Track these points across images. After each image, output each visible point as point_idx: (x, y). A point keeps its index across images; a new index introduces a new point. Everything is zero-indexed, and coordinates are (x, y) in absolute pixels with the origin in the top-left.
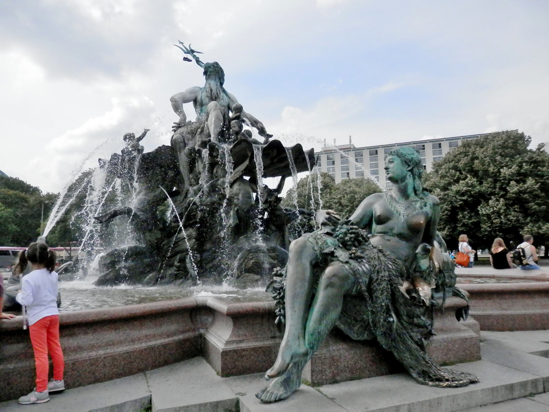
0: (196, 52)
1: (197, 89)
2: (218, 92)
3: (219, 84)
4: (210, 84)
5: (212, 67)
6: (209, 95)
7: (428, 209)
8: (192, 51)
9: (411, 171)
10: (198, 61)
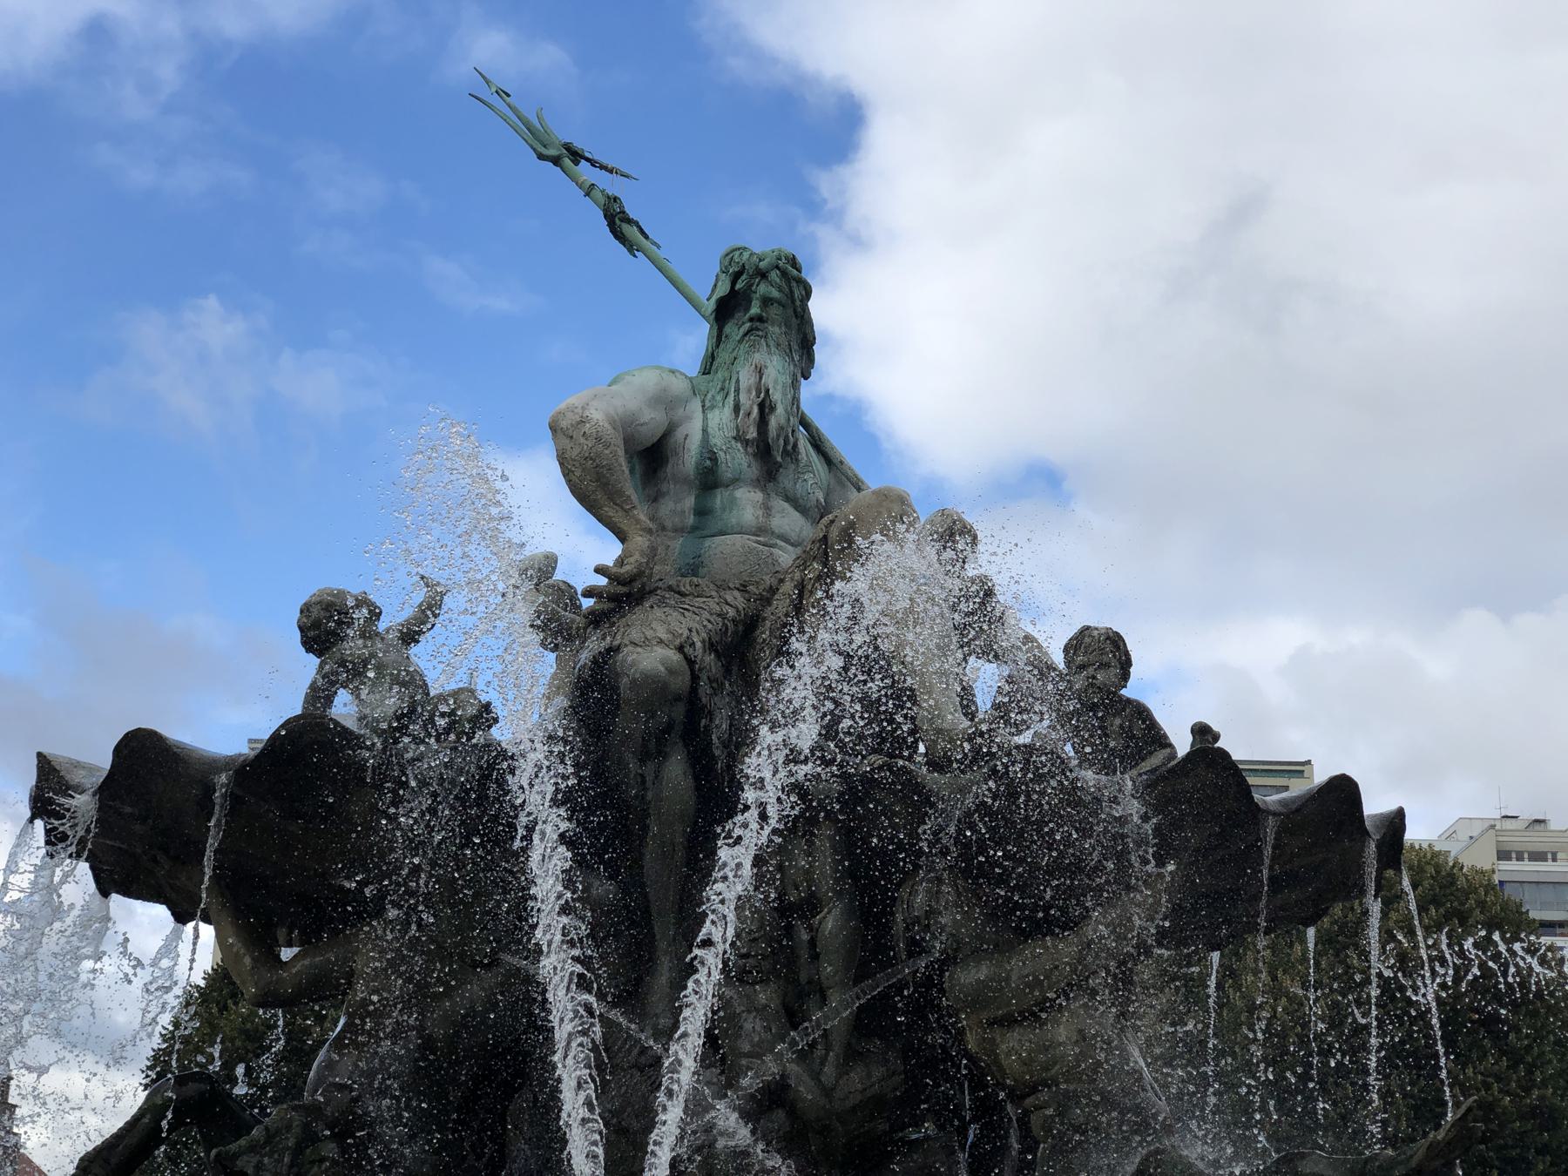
0: (592, 162)
4: (760, 372)
5: (774, 276)
6: (752, 434)
8: (576, 156)
10: (617, 220)
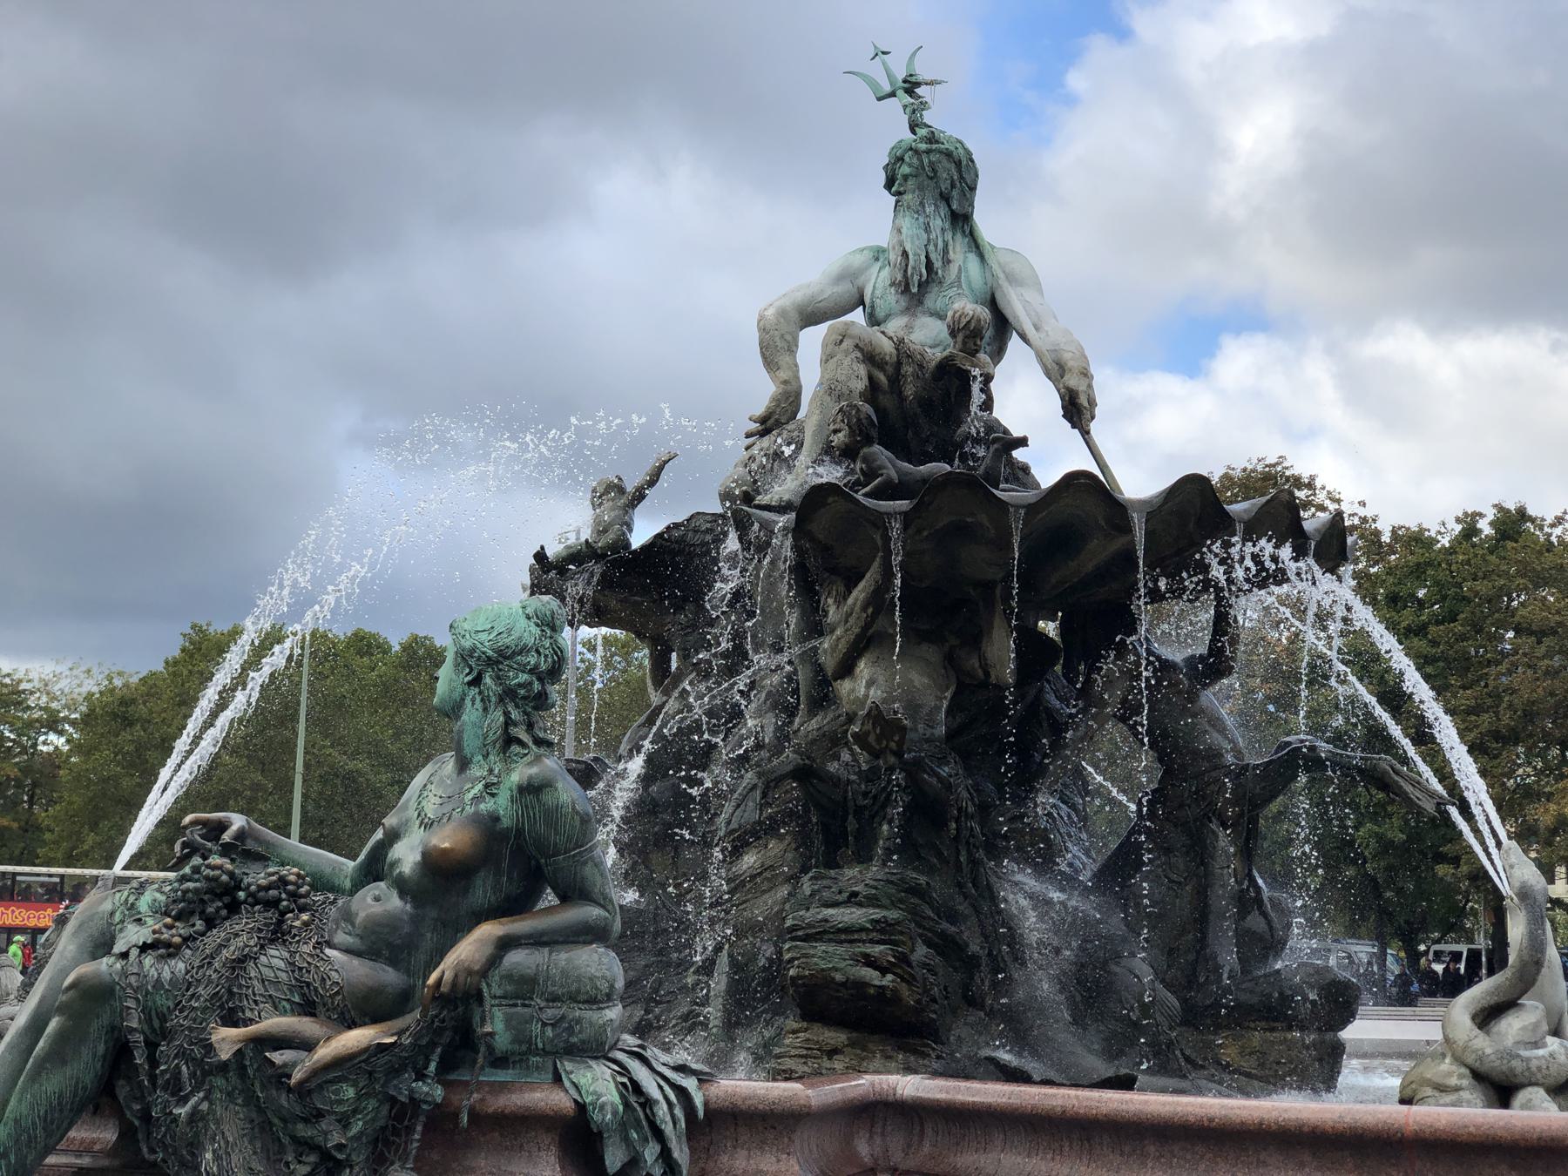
1: (858, 260)
2: (933, 256)
3: (937, 223)
4: (899, 231)
6: (899, 277)
7: (501, 804)
9: (477, 681)
